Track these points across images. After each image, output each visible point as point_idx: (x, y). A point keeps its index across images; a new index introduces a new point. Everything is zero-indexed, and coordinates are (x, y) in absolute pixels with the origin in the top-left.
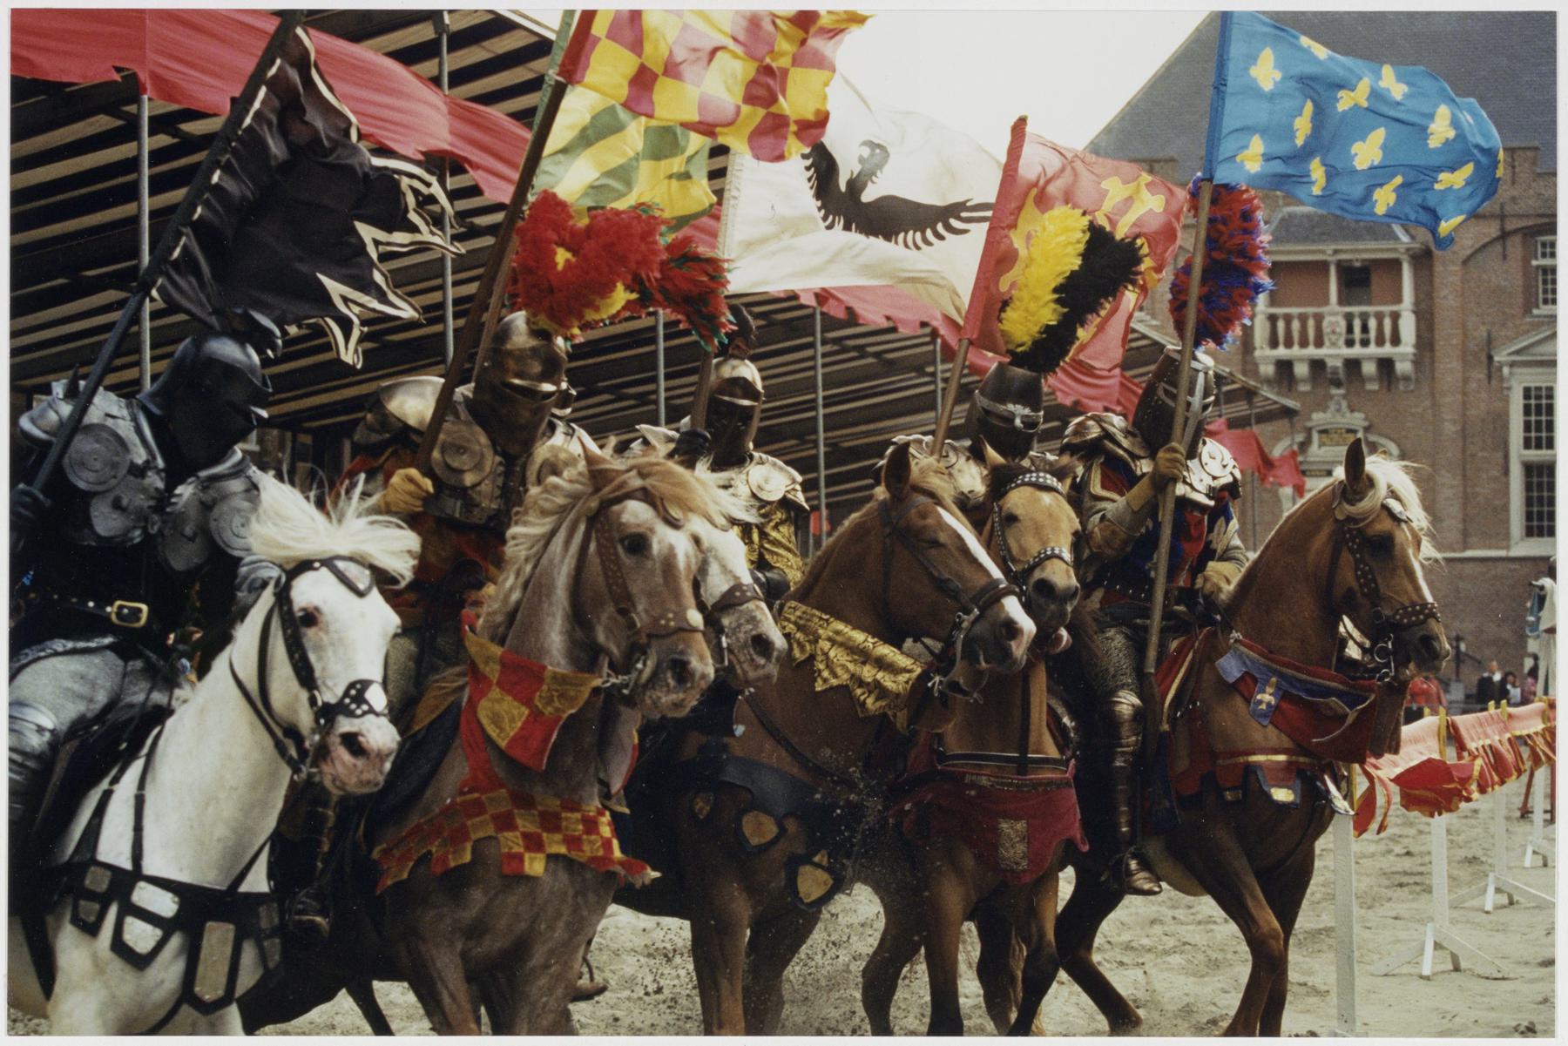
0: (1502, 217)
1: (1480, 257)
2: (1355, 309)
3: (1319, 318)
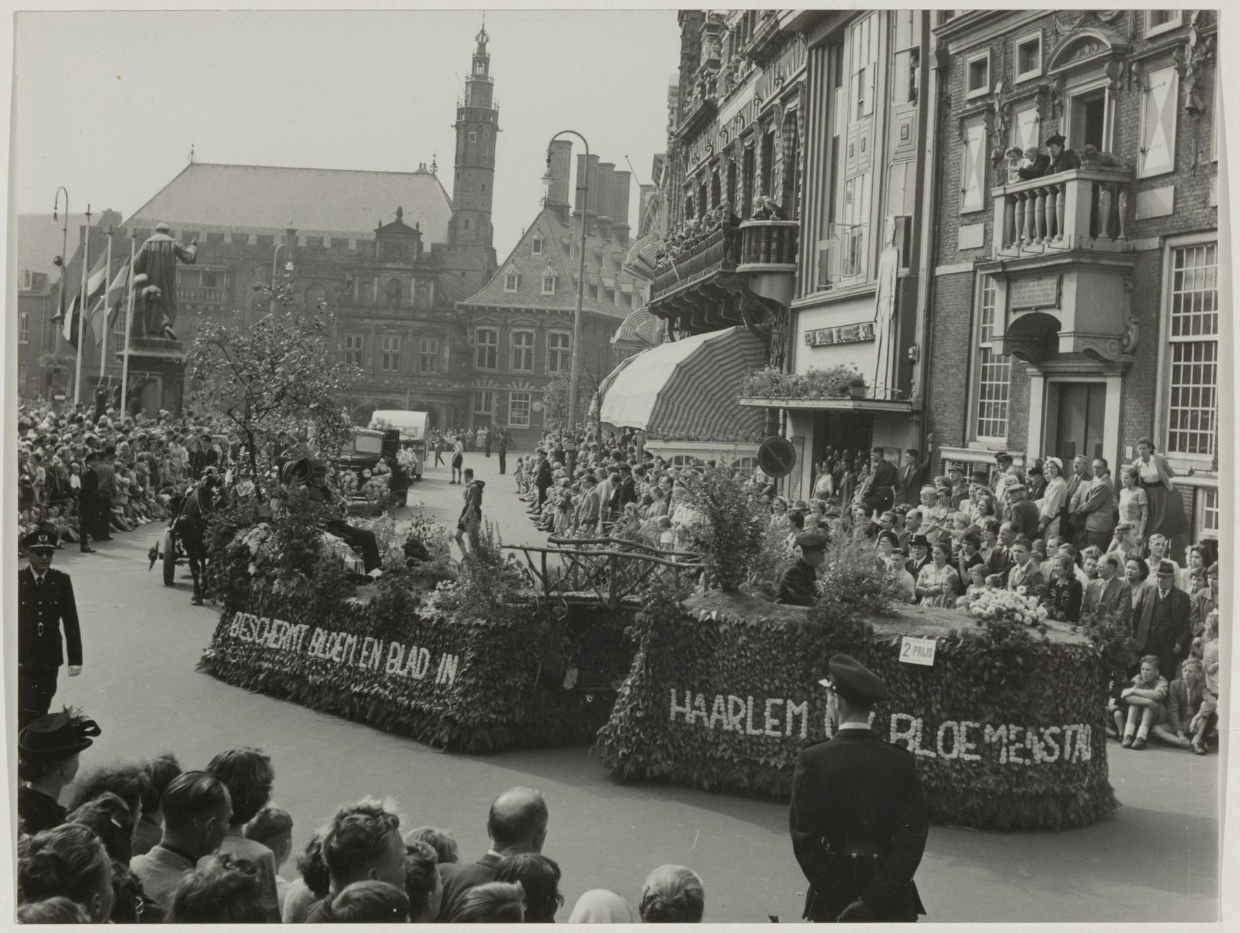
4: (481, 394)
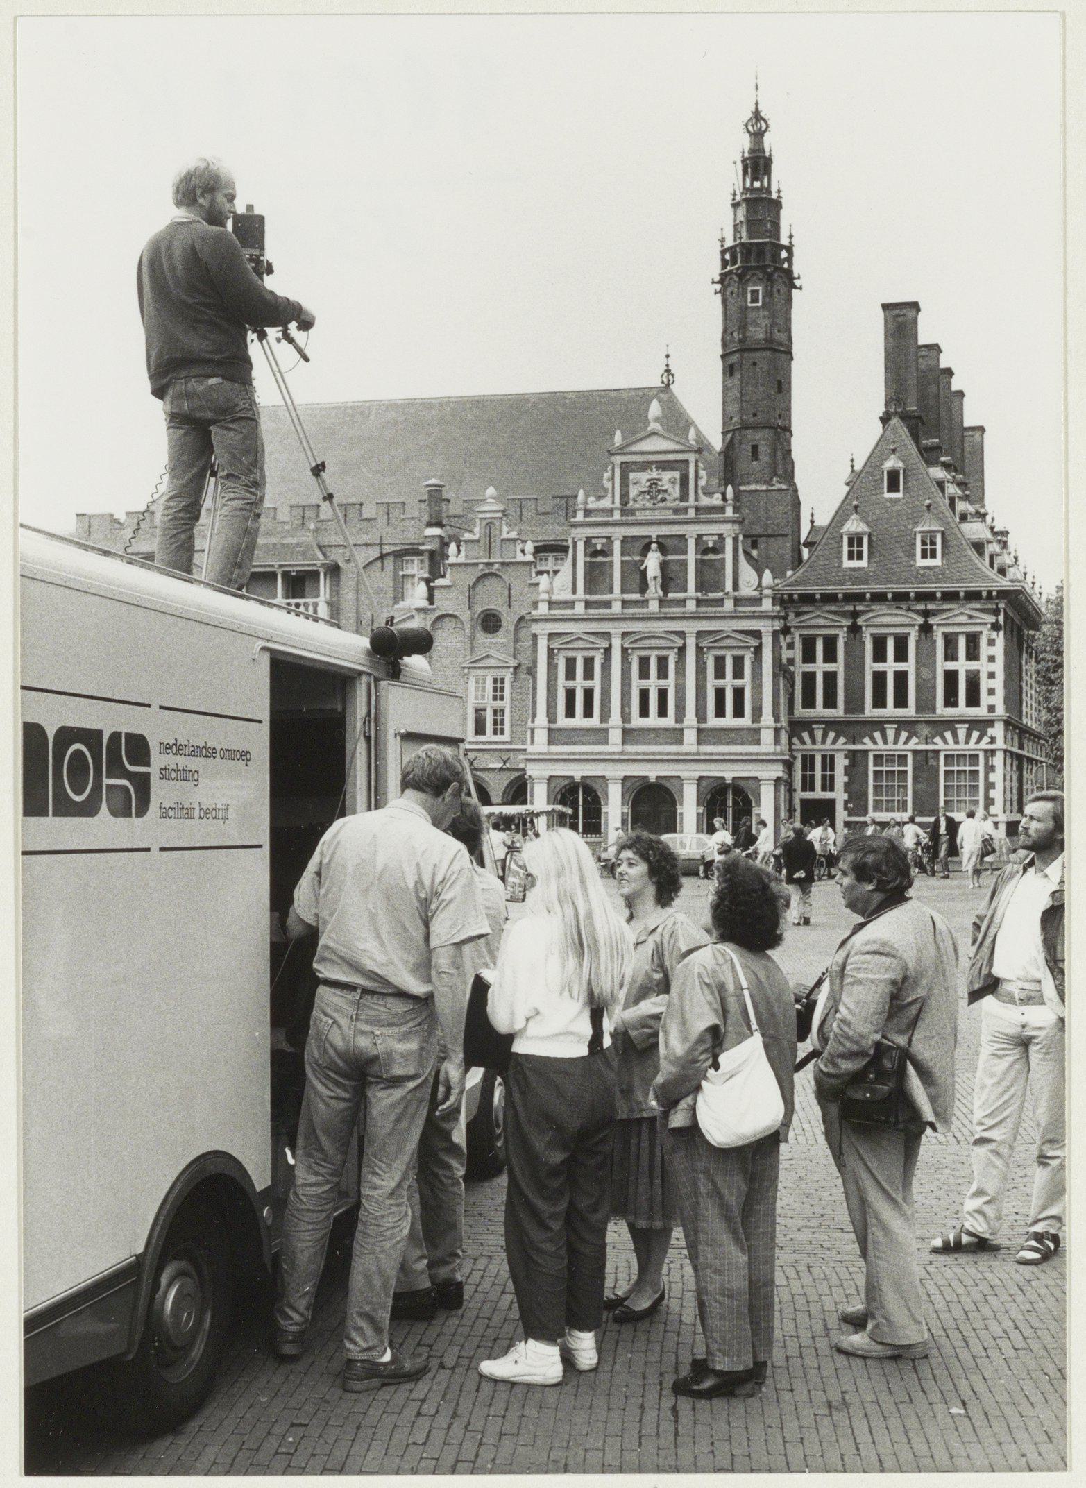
4: (813, 757)
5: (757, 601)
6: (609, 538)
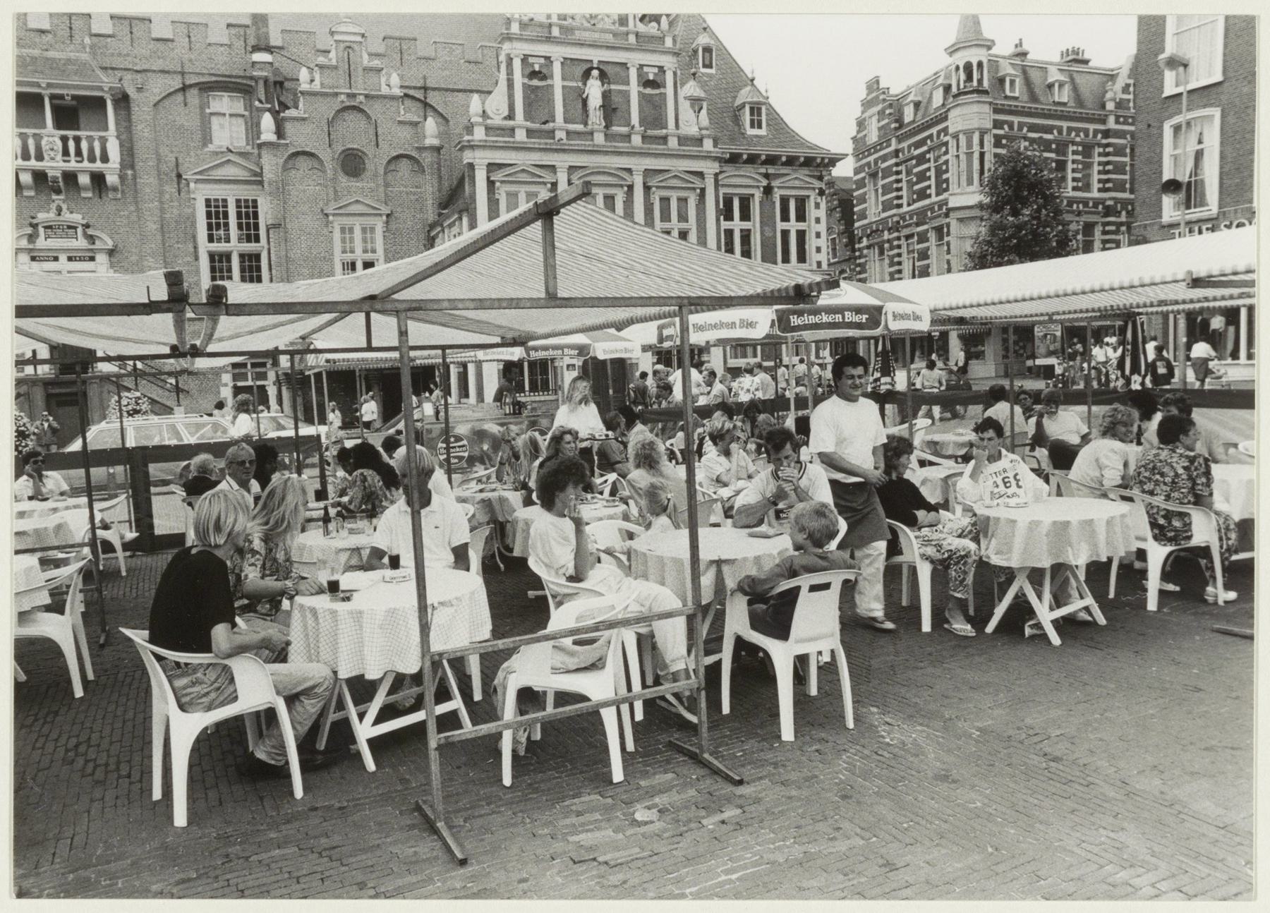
0: (183, 74)
1: (167, 103)
2: (70, 133)
3: (38, 138)
5: (699, 141)
6: (547, 58)
